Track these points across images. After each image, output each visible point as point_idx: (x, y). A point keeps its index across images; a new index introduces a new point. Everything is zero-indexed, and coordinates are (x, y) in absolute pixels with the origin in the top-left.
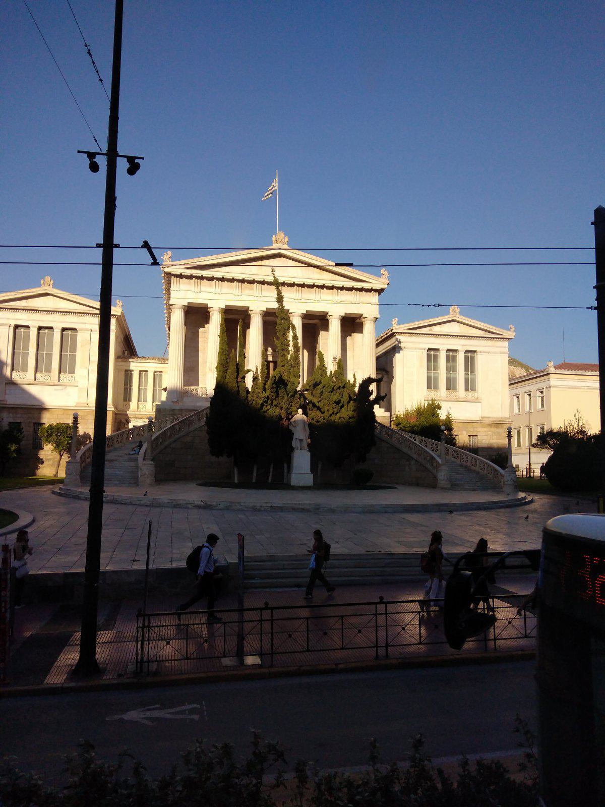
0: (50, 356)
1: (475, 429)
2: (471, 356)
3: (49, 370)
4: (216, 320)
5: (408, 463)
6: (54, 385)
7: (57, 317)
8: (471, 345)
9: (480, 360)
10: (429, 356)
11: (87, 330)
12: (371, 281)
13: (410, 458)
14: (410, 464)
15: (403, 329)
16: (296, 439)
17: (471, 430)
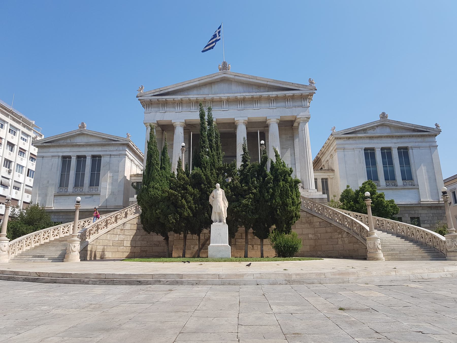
0: (83, 175)
1: (417, 212)
2: (404, 153)
3: (82, 185)
4: (179, 132)
5: (340, 235)
6: (85, 195)
7: (89, 149)
8: (403, 143)
9: (414, 155)
10: (366, 155)
11: (107, 155)
12: (300, 89)
13: (341, 232)
14: (342, 237)
15: (340, 134)
16: (215, 213)
17: (413, 212)
